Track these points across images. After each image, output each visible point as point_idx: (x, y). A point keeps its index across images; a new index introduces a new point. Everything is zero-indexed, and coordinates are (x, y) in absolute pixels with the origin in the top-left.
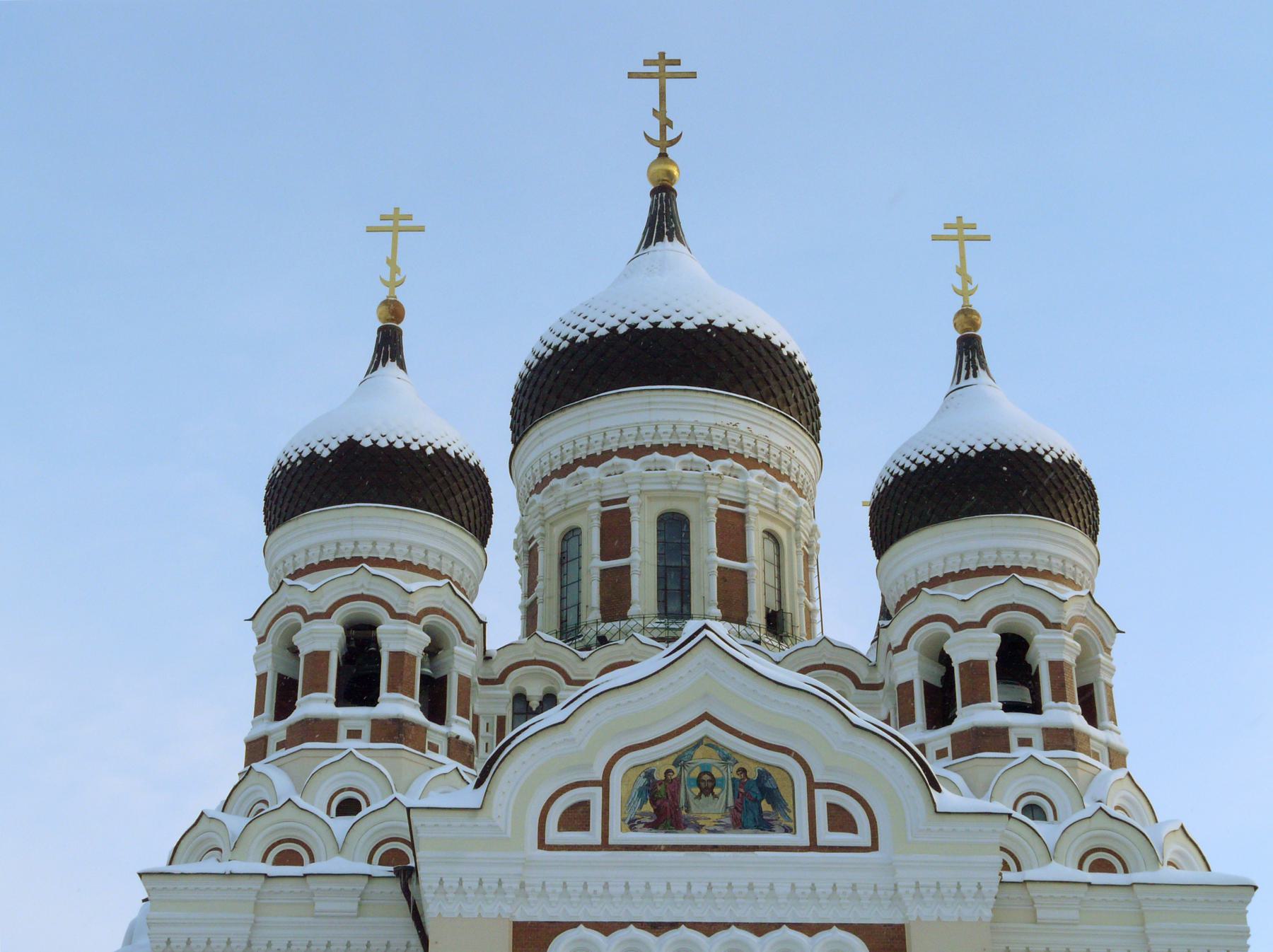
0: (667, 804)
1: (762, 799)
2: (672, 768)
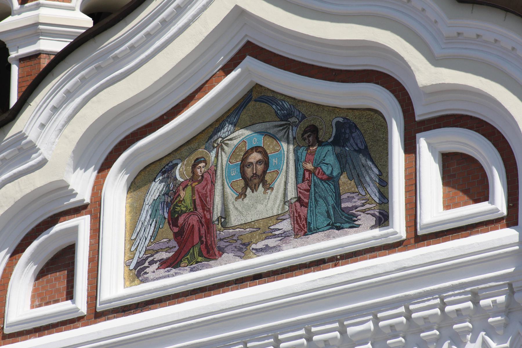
0: (194, 220)
1: (341, 174)
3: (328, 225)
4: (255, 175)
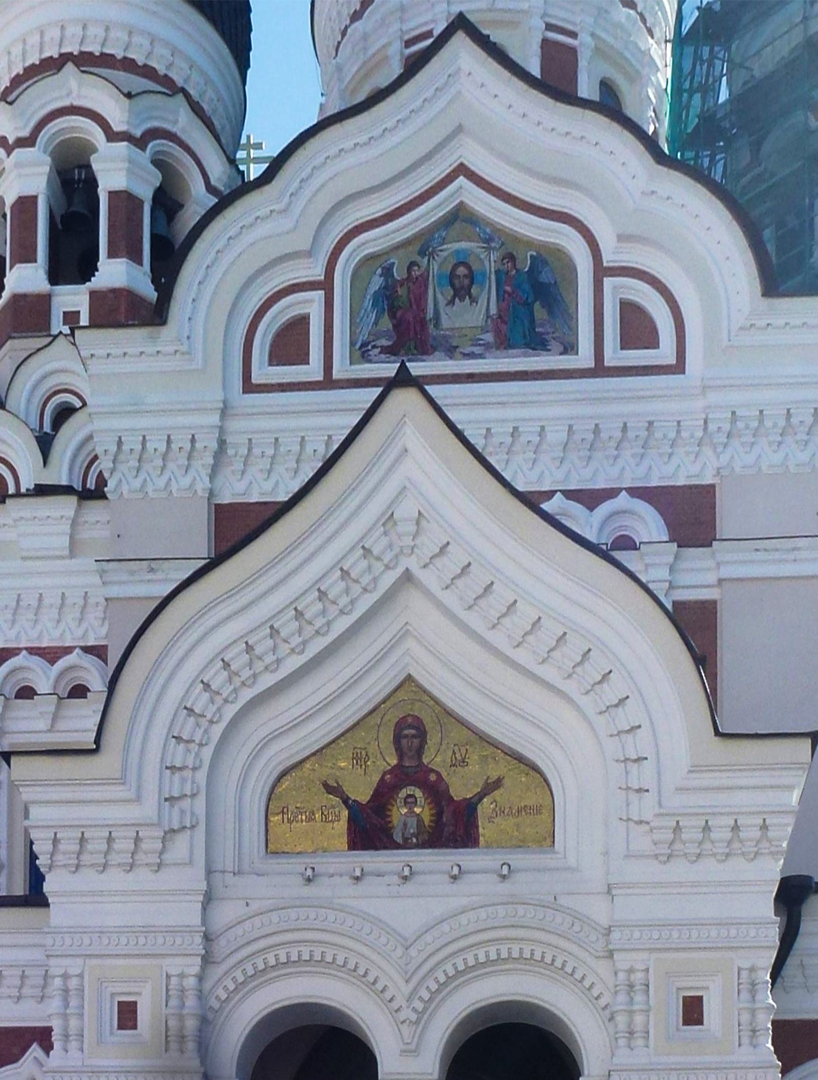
0: (410, 317)
2: (418, 259)
3: (525, 344)
4: (462, 288)
